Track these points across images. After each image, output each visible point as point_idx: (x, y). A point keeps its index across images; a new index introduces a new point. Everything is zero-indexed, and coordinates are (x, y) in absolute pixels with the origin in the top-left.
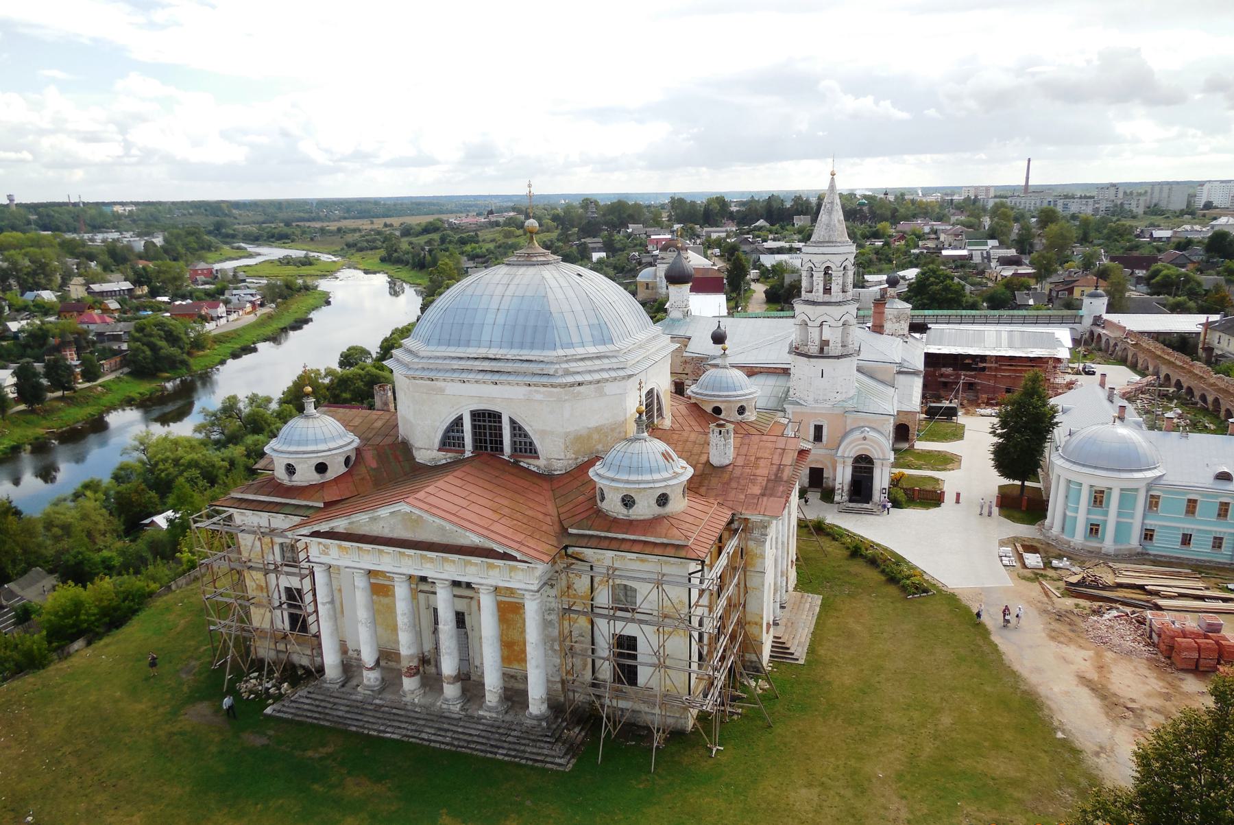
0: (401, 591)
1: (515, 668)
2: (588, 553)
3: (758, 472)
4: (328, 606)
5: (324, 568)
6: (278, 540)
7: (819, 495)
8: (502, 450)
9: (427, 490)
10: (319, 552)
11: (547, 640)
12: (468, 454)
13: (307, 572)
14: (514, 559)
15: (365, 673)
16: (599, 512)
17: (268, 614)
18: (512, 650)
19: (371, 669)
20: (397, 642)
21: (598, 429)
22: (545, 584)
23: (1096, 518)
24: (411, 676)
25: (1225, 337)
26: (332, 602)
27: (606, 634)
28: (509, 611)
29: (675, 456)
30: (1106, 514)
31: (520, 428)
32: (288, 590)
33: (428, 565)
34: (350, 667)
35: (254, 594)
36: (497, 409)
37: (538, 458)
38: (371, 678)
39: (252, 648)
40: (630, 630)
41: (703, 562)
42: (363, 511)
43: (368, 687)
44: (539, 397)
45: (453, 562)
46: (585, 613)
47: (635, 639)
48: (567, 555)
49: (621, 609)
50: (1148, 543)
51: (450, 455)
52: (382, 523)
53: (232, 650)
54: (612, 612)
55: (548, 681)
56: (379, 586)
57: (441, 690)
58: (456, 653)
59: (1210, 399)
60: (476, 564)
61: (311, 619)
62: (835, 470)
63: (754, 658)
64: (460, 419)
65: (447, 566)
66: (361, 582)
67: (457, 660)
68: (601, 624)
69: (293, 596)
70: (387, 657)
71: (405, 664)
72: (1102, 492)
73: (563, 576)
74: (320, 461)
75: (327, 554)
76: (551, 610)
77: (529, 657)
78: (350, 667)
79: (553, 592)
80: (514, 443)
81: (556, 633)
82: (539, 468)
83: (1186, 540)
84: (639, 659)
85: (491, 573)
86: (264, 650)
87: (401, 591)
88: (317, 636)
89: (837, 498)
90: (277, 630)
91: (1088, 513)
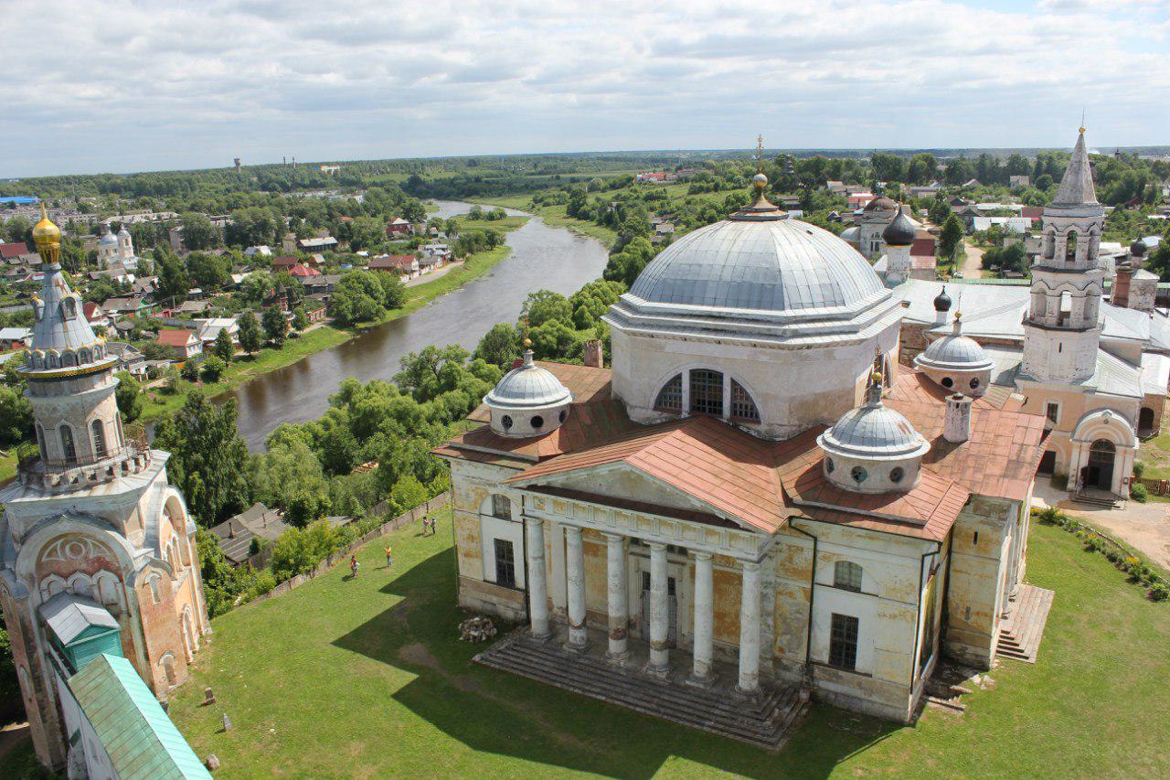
0: (614, 551)
1: (726, 640)
3: (998, 451)
4: (539, 561)
8: (721, 412)
9: (647, 449)
15: (572, 632)
18: (726, 622)
19: (579, 628)
21: (825, 396)
22: (765, 555)
24: (617, 638)
28: (726, 580)
31: (742, 390)
34: (556, 625)
36: (719, 369)
37: (759, 422)
38: (576, 636)
43: (574, 646)
44: (764, 358)
51: (665, 415)
55: (761, 657)
56: (592, 545)
57: (648, 655)
58: (666, 620)
63: (981, 652)
64: (679, 377)
66: (573, 540)
67: (666, 627)
70: (594, 618)
71: (613, 626)
74: (536, 414)
75: (541, 508)
77: (743, 630)
78: (556, 625)
80: (734, 406)
82: (759, 432)
87: (614, 551)
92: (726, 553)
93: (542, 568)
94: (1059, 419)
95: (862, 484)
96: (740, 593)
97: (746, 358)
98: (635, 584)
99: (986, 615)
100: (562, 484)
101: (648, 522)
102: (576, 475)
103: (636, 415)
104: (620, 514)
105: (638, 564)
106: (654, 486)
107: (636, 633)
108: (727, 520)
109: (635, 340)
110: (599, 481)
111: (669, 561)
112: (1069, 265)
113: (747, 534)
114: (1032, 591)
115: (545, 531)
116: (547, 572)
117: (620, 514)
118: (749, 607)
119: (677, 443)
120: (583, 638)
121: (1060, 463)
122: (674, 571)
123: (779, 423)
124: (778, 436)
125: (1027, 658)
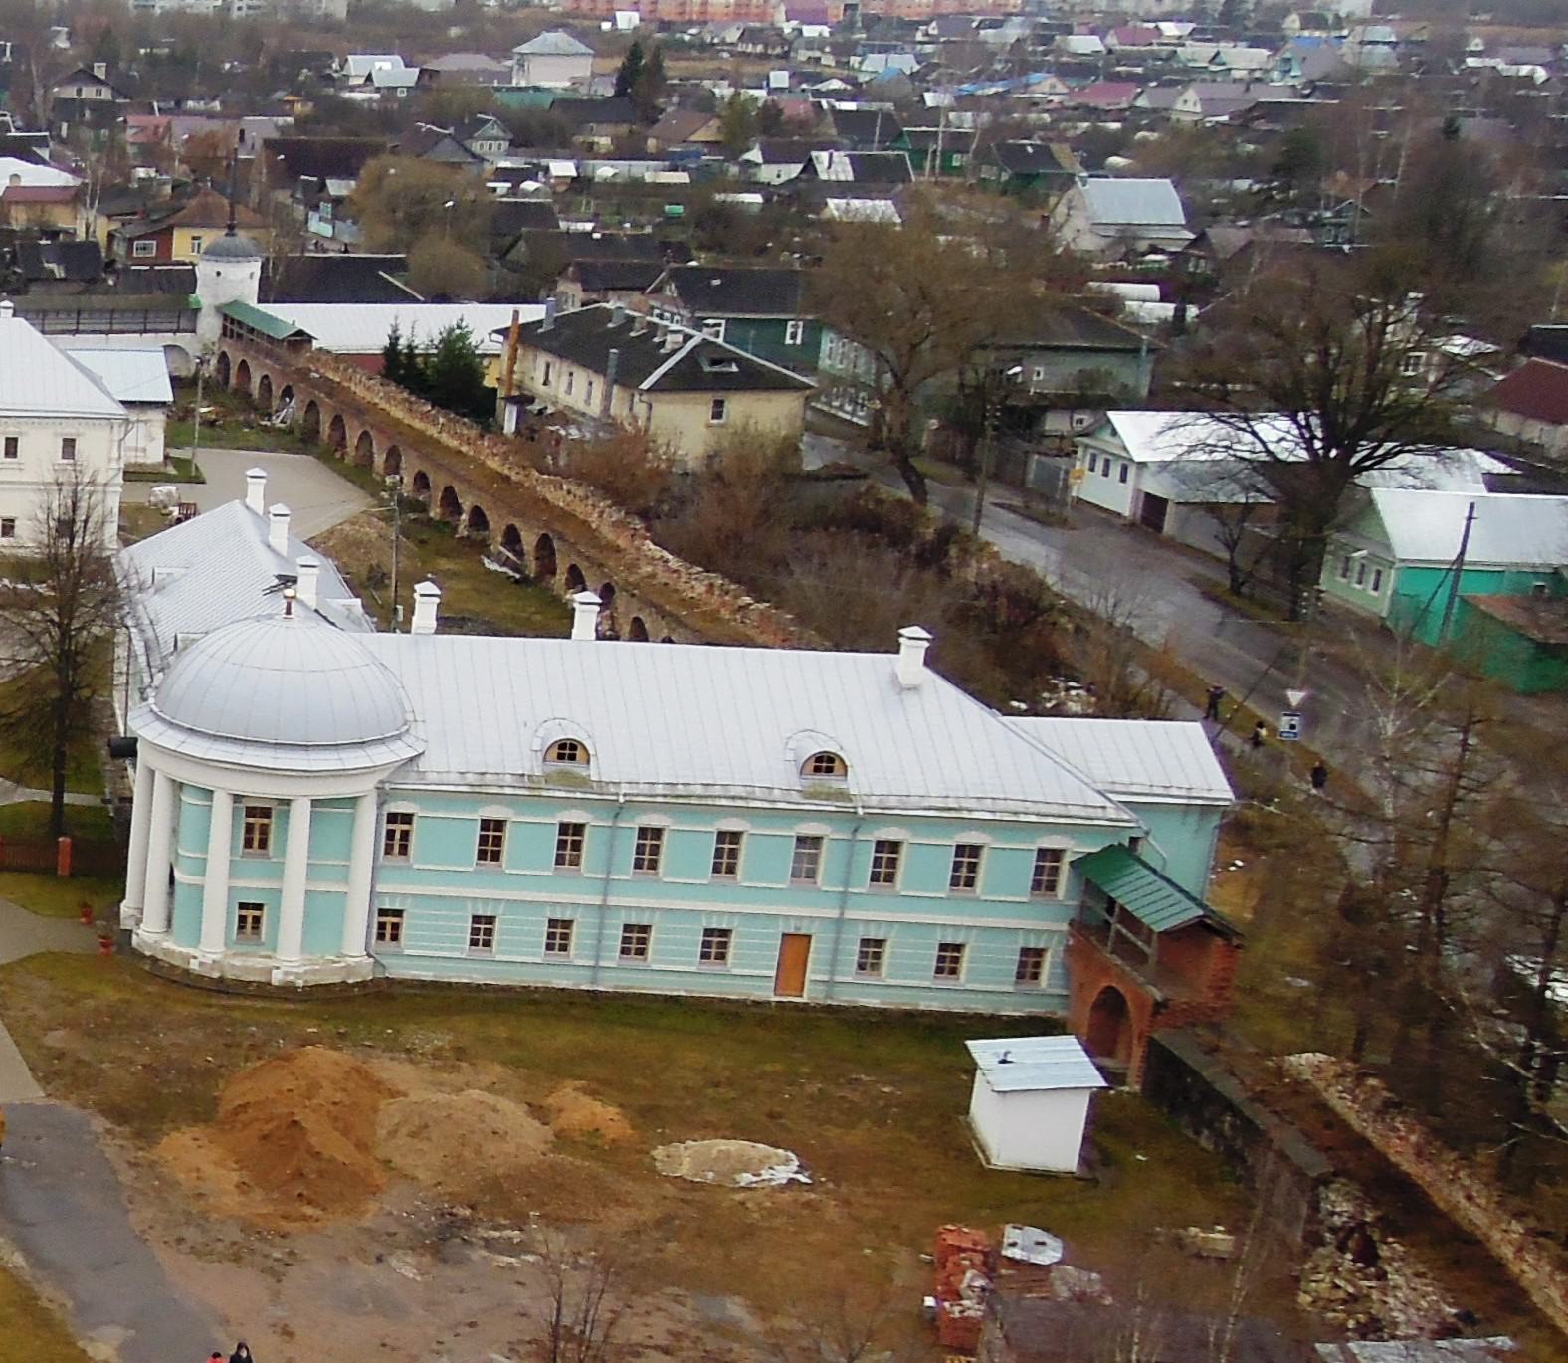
23: (253, 886)
25: (560, 370)
30: (279, 872)
50: (388, 945)
59: (529, 540)
72: (266, 813)
83: (482, 930)
91: (232, 875)
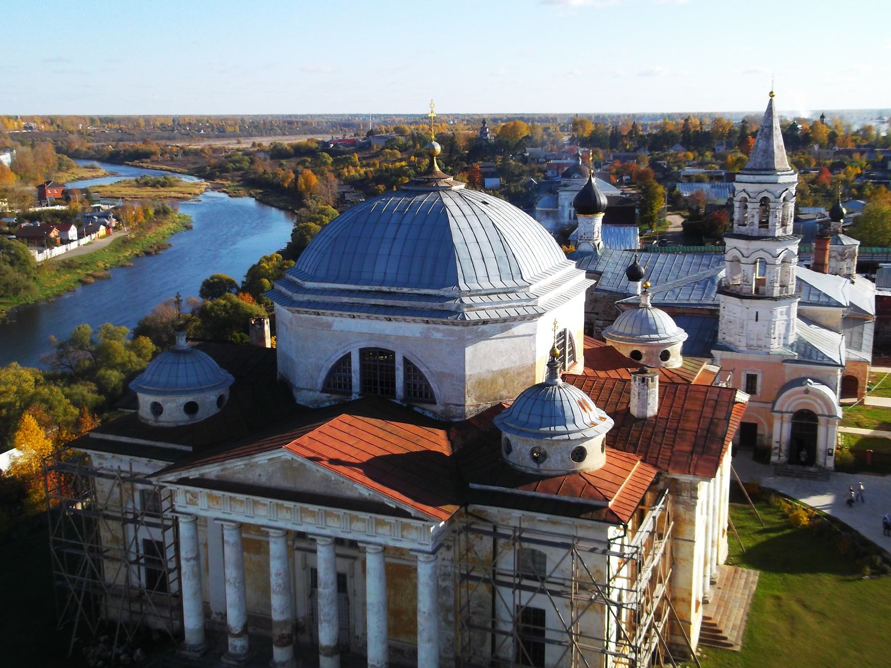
0: (276, 547)
2: (493, 511)
4: (192, 562)
5: (190, 519)
6: (140, 486)
7: (751, 454)
9: (310, 434)
10: (184, 500)
11: (441, 608)
12: (355, 397)
13: (169, 523)
14: (407, 515)
15: (231, 640)
16: (505, 465)
17: (124, 570)
18: (401, 620)
20: (269, 606)
22: (441, 546)
24: (282, 645)
26: (197, 558)
27: (510, 606)
28: (399, 574)
29: (592, 405)
32: (148, 544)
33: (309, 520)
35: (109, 545)
36: (390, 347)
38: (237, 645)
39: (102, 608)
40: (539, 602)
41: (626, 527)
42: (238, 456)
43: (234, 656)
44: (438, 335)
45: (338, 517)
46: (486, 581)
47: (542, 612)
48: (467, 513)
49: (528, 578)
51: (334, 396)
52: (258, 471)
53: (80, 608)
54: (517, 580)
55: (440, 657)
58: (335, 622)
60: (363, 520)
61: (172, 576)
62: (771, 426)
64: (348, 357)
65: (330, 522)
66: (230, 536)
67: (336, 629)
68: (506, 593)
69: (154, 549)
70: (257, 622)
71: (277, 632)
73: (463, 537)
75: (195, 504)
76: (446, 576)
77: (420, 628)
79: (449, 555)
81: (451, 602)
84: (548, 635)
85: (381, 530)
86: (116, 610)
87: (276, 547)
88: (179, 596)
89: (774, 458)
90: (132, 587)
92: (398, 545)
93: (196, 569)
94: (759, 389)
95: (541, 466)
96: (415, 587)
97: (418, 335)
98: (302, 584)
99: (684, 600)
100: (217, 476)
101: (313, 514)
102: (232, 465)
103: (303, 398)
104: (281, 506)
105: (306, 560)
106: (318, 474)
107: (305, 638)
108: (398, 509)
109: (301, 318)
110: (258, 471)
111: (338, 555)
112: (763, 231)
113: (419, 523)
114: (736, 572)
115: (199, 528)
116: (203, 573)
117: (281, 506)
118: (425, 602)
119: (345, 427)
120: (243, 647)
121: (762, 435)
122: (344, 566)
123: (455, 402)
124: (453, 417)
125: (731, 645)
